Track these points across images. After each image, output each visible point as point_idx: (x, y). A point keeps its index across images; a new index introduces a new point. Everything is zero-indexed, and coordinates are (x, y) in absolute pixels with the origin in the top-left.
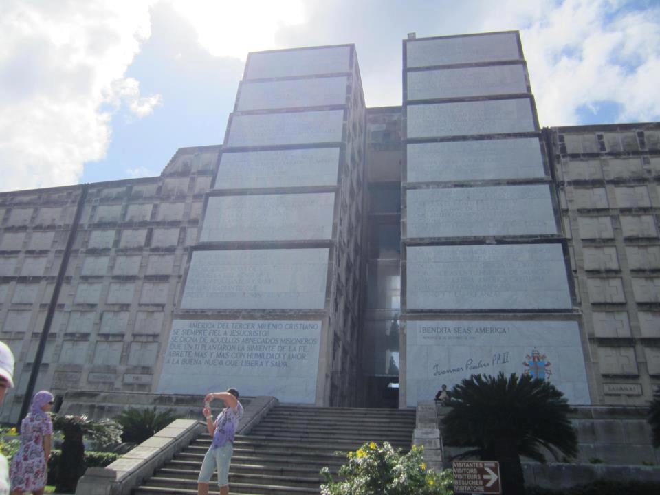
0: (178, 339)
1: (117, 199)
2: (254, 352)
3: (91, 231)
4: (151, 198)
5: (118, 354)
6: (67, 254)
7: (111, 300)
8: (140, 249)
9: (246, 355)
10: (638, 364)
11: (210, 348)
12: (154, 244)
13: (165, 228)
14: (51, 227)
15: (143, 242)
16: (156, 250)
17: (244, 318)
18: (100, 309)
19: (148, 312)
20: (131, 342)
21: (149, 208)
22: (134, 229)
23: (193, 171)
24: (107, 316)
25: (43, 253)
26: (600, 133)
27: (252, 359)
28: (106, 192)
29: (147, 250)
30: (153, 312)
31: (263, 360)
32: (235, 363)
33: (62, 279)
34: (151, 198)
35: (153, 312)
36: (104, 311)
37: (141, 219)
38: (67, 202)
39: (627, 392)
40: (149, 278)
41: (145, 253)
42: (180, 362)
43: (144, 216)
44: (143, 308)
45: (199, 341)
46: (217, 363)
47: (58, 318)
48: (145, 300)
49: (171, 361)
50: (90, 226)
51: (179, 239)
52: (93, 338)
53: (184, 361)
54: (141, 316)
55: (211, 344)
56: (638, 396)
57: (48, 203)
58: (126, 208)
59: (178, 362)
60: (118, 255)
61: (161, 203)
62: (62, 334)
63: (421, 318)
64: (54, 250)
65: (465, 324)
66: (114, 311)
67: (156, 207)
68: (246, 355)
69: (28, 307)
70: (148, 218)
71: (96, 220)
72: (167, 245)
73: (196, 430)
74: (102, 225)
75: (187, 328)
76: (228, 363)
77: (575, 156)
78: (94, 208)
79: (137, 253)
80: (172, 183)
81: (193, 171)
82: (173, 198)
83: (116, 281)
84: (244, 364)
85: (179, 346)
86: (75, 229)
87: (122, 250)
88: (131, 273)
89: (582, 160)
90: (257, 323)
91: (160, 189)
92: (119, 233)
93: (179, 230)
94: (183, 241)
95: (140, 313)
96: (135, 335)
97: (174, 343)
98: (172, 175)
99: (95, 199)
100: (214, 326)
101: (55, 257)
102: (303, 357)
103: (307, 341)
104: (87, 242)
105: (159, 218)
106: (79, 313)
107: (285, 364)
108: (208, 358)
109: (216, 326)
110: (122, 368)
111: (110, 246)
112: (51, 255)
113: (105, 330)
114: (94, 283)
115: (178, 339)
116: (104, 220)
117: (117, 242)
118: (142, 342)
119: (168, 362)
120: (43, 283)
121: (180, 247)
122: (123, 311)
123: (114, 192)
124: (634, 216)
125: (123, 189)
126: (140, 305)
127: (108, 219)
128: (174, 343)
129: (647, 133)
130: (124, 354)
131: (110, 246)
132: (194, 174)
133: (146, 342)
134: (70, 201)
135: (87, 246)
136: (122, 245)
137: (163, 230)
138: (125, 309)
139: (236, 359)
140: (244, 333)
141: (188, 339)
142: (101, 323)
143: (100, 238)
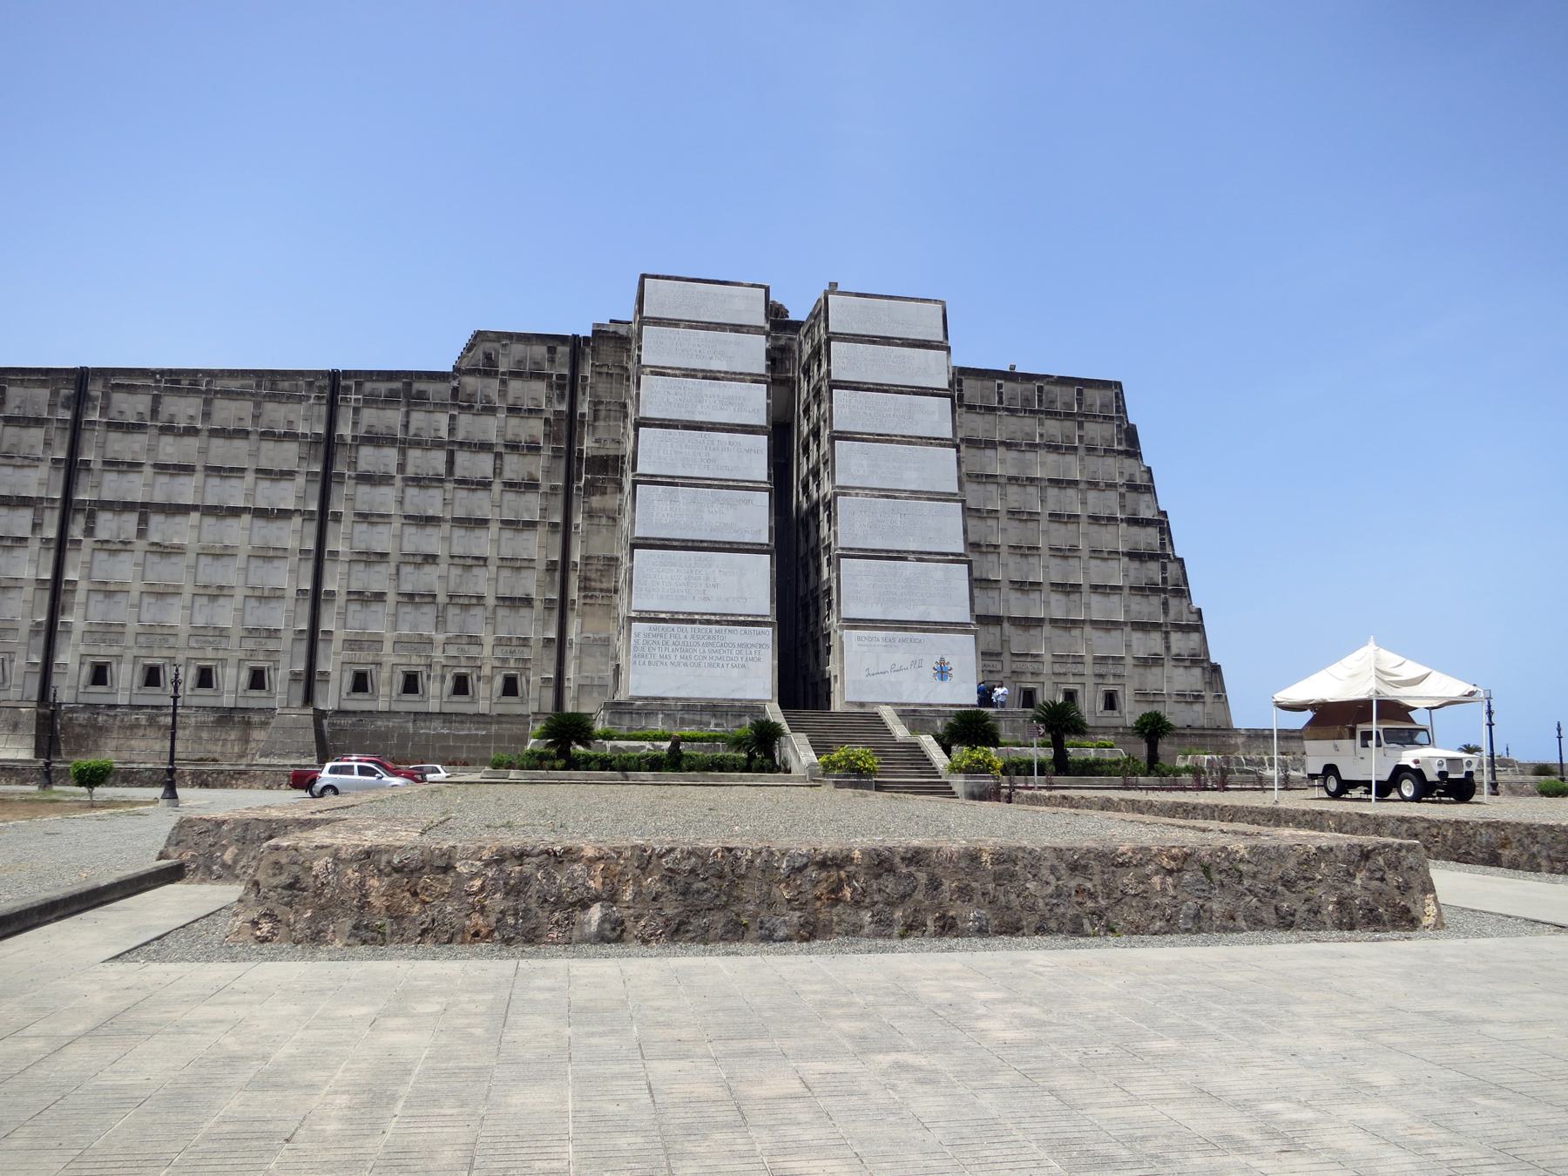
0: (641, 642)
3: (357, 446)
6: (327, 481)
7: (408, 548)
10: (1003, 641)
12: (459, 473)
13: (471, 452)
16: (462, 482)
17: (701, 622)
21: (442, 420)
22: (423, 449)
24: (406, 570)
26: (1000, 382)
28: (368, 386)
29: (450, 481)
30: (471, 566)
33: (323, 518)
37: (433, 434)
38: (309, 398)
39: (988, 669)
40: (460, 522)
43: (437, 430)
44: (456, 561)
48: (457, 551)
50: (354, 438)
51: (495, 469)
52: (391, 598)
54: (456, 572)
56: (999, 672)
57: (274, 397)
58: (407, 414)
60: (407, 485)
62: (344, 591)
63: (855, 628)
64: (304, 469)
65: (891, 634)
66: (415, 563)
67: (452, 418)
69: (280, 553)
71: (361, 431)
72: (477, 475)
74: (374, 439)
77: (971, 408)
78: (356, 410)
79: (435, 484)
80: (471, 383)
88: (430, 513)
89: (978, 413)
91: (455, 391)
92: (403, 452)
94: (501, 473)
98: (470, 372)
102: (759, 660)
103: (761, 646)
104: (355, 463)
105: (460, 437)
107: (743, 666)
110: (440, 637)
112: (300, 480)
113: (407, 588)
115: (641, 642)
116: (374, 430)
117: (402, 467)
120: (297, 521)
121: (497, 480)
123: (383, 387)
124: (1019, 485)
125: (397, 385)
126: (452, 557)
127: (381, 429)
129: (1046, 388)
130: (440, 619)
134: (313, 396)
136: (410, 471)
137: (468, 454)
138: (430, 561)
142: (398, 578)
143: (368, 458)
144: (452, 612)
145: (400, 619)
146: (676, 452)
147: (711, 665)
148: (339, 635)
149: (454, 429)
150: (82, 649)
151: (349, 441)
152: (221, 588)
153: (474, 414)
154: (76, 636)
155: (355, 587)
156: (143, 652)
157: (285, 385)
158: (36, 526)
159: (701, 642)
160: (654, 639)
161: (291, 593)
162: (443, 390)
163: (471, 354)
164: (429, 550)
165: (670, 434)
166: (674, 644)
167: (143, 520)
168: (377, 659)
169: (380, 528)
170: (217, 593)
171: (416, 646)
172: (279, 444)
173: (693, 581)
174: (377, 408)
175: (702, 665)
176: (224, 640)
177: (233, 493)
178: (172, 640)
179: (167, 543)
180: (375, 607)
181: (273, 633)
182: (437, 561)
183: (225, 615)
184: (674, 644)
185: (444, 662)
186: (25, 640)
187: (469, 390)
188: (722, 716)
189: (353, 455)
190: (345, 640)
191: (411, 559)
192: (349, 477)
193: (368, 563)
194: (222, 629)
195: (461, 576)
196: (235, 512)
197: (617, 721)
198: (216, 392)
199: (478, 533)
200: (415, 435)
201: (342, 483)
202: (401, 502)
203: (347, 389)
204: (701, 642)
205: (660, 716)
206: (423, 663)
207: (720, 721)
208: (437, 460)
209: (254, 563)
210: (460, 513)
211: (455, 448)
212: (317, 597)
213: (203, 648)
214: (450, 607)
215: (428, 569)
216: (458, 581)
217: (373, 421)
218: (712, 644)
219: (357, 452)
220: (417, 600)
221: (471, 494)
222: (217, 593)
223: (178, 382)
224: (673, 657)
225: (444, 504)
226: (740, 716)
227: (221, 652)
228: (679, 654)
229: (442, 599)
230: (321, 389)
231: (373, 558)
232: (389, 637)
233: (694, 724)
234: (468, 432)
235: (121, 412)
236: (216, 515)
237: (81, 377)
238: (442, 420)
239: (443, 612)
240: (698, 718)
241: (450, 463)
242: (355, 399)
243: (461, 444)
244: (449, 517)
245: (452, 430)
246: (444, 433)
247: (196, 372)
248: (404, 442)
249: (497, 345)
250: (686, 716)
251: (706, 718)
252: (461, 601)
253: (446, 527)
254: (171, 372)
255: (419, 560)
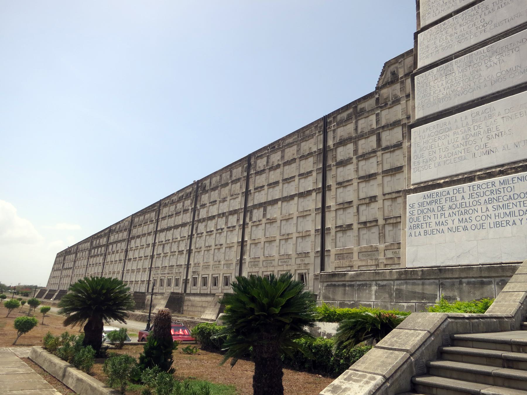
0: (416, 213)
1: (349, 118)
2: (501, 211)
3: (336, 149)
4: (373, 110)
5: (376, 235)
7: (362, 196)
8: (374, 152)
9: (493, 217)
11: (450, 215)
12: (384, 144)
13: (390, 130)
14: (310, 154)
15: (375, 146)
16: (387, 148)
17: (480, 178)
18: (355, 204)
19: (392, 199)
20: (384, 225)
21: (373, 118)
22: (365, 138)
23: (400, 76)
24: (362, 208)
25: (309, 173)
27: (500, 220)
28: (339, 117)
29: (379, 151)
30: (396, 198)
31: (515, 218)
32: (482, 226)
33: (324, 189)
34: (373, 110)
35: (396, 198)
36: (359, 205)
37: (369, 128)
41: (379, 153)
42: (422, 233)
43: (371, 125)
44: (387, 197)
45: (436, 210)
46: (461, 229)
47: (330, 217)
48: (387, 190)
49: (413, 234)
50: (334, 145)
51: (403, 134)
52: (355, 226)
53: (426, 232)
54: (388, 203)
55: (451, 211)
58: (356, 123)
59: (420, 234)
60: (359, 161)
61: (381, 111)
64: (315, 169)
66: (366, 204)
67: (377, 115)
68: (493, 217)
70: (374, 126)
71: (338, 140)
72: (394, 142)
73: (444, 330)
74: (343, 142)
75: (422, 200)
76: (473, 228)
78: (334, 131)
79: (372, 155)
80: (385, 92)
81: (400, 76)
82: (389, 103)
83: (362, 180)
84: (492, 225)
85: (418, 219)
86: (325, 152)
87: (361, 156)
88: (372, 172)
90: (496, 179)
91: (378, 99)
93: (401, 127)
95: (385, 201)
96: (386, 220)
97: (413, 217)
98: (384, 86)
99: (333, 124)
100: (448, 193)
101: (317, 174)
104: (335, 157)
105: (383, 123)
106: (342, 210)
108: (450, 225)
109: (451, 193)
110: (382, 246)
111: (352, 155)
113: (363, 219)
114: (347, 186)
115: (416, 213)
117: (356, 151)
118: (393, 223)
119: (411, 235)
120: (314, 194)
122: (372, 202)
123: (345, 115)
125: (351, 110)
127: (346, 136)
128: (413, 217)
130: (381, 235)
131: (352, 155)
132: (402, 78)
133: (396, 223)
134: (317, 132)
135: (336, 161)
136: (360, 152)
137: (388, 131)
138: (373, 200)
139: (481, 222)
140: (484, 193)
141: (425, 211)
142: (358, 214)
143: (343, 153)
144: (388, 228)
145: (361, 238)
146: (451, 36)
147: (498, 225)
148: (333, 252)
149: (379, 120)
150: (249, 270)
151: (332, 148)
152: (288, 234)
153: (389, 108)
154: (247, 263)
155: (339, 223)
156: (264, 269)
157: (307, 132)
158: (238, 220)
159: (482, 200)
160: (429, 207)
161: (313, 232)
162: (372, 102)
163: (383, 77)
164: (372, 194)
165: (444, 24)
166: (450, 208)
167: (265, 210)
168: (351, 264)
169: (349, 188)
170: (287, 238)
171: (370, 253)
172: (307, 160)
173: (472, 139)
174: (343, 126)
175: (486, 226)
176: (290, 260)
177: (291, 189)
178: (273, 262)
179: (271, 218)
180: (349, 233)
181: (307, 254)
182: (377, 200)
183: (289, 248)
184: (450, 208)
185: (385, 262)
186: (234, 268)
187: (385, 96)
188: (453, 284)
189: (334, 154)
190: (335, 254)
191: (363, 202)
192: (333, 166)
193: (344, 209)
194: (289, 255)
195: (391, 205)
196: (292, 197)
197: (331, 296)
198: (285, 146)
199: (398, 176)
200: (361, 132)
201: (331, 170)
202: (357, 171)
203: (330, 122)
204: (482, 200)
205: (374, 288)
206: (374, 264)
207: (450, 294)
208: (372, 141)
209: (300, 220)
210: (387, 167)
211: (380, 131)
212: (323, 232)
213: (283, 265)
214: (386, 226)
215: (373, 205)
216: (390, 209)
217: (342, 134)
218: (498, 200)
219: (336, 152)
220: (368, 225)
221: (392, 154)
222: (287, 238)
223: (274, 147)
224: (450, 222)
225: (378, 165)
226: (482, 283)
227: (289, 266)
228: (456, 218)
229: (381, 222)
230: (320, 127)
231: (346, 206)
232: (356, 249)
233: (414, 298)
234: (387, 120)
235: (259, 167)
236: (286, 201)
237: (248, 158)
238: (373, 118)
239: (382, 230)
240: (418, 289)
241: (379, 140)
242: (333, 126)
243: (383, 127)
244: (381, 171)
245: (377, 122)
246: (374, 126)
247: (279, 140)
248: (356, 138)
249: (397, 65)
250: (404, 287)
251: (429, 289)
252: (391, 221)
253: (379, 178)
254: (272, 144)
255: (367, 201)
